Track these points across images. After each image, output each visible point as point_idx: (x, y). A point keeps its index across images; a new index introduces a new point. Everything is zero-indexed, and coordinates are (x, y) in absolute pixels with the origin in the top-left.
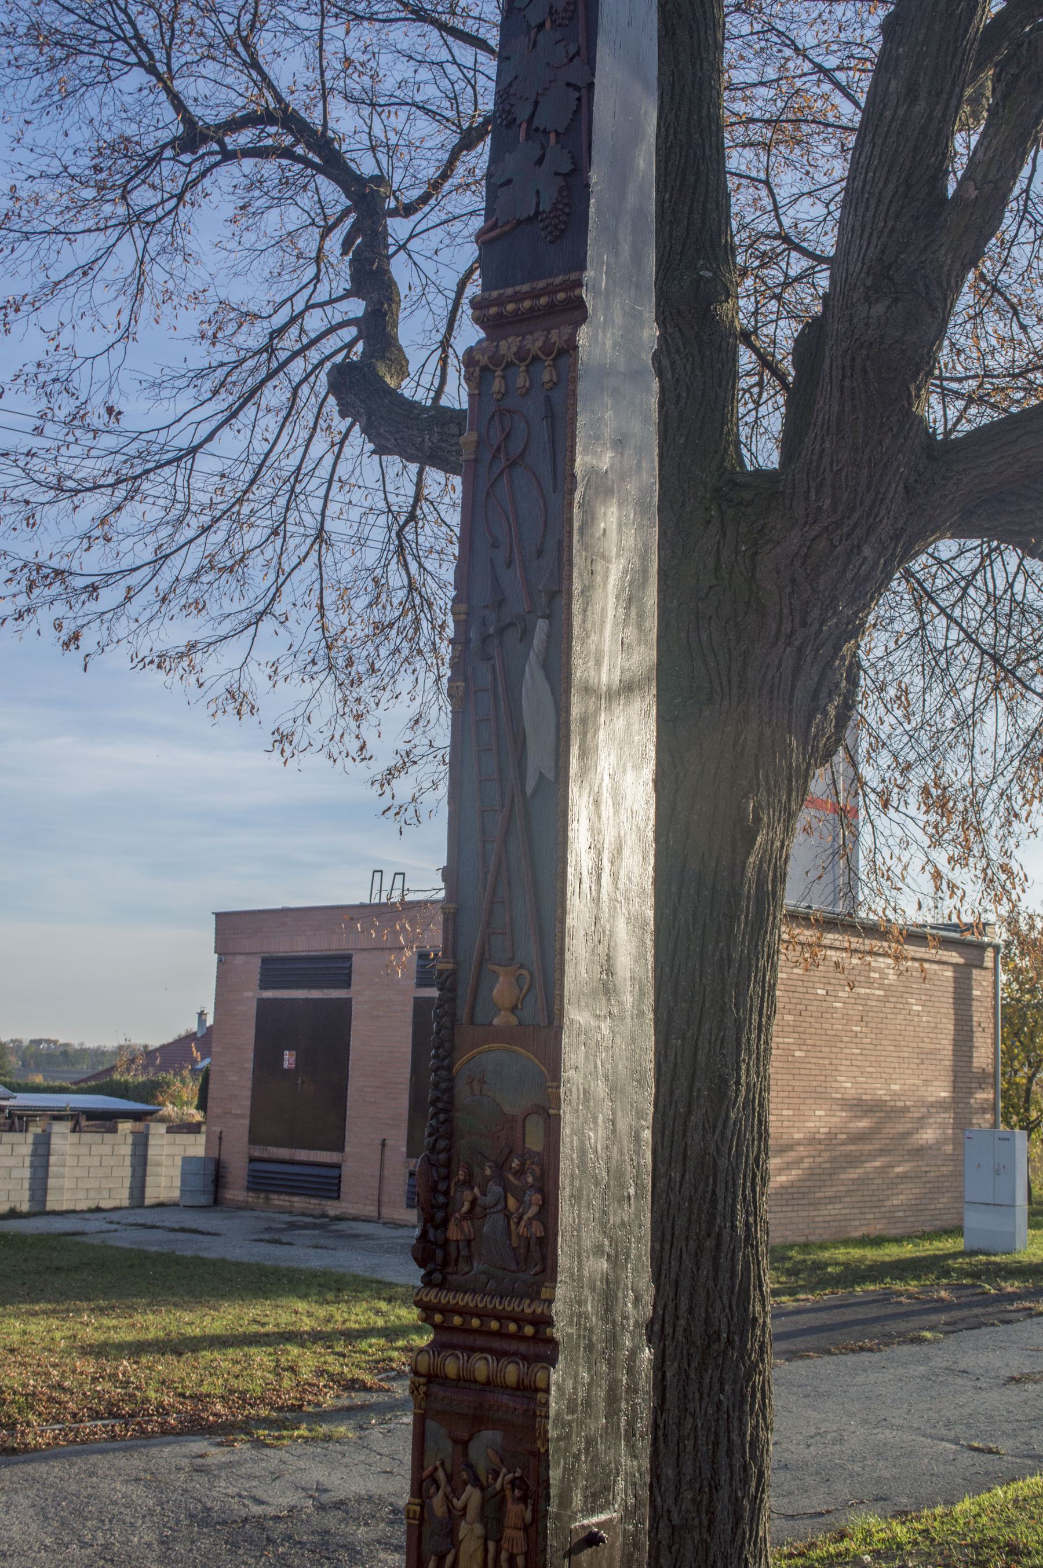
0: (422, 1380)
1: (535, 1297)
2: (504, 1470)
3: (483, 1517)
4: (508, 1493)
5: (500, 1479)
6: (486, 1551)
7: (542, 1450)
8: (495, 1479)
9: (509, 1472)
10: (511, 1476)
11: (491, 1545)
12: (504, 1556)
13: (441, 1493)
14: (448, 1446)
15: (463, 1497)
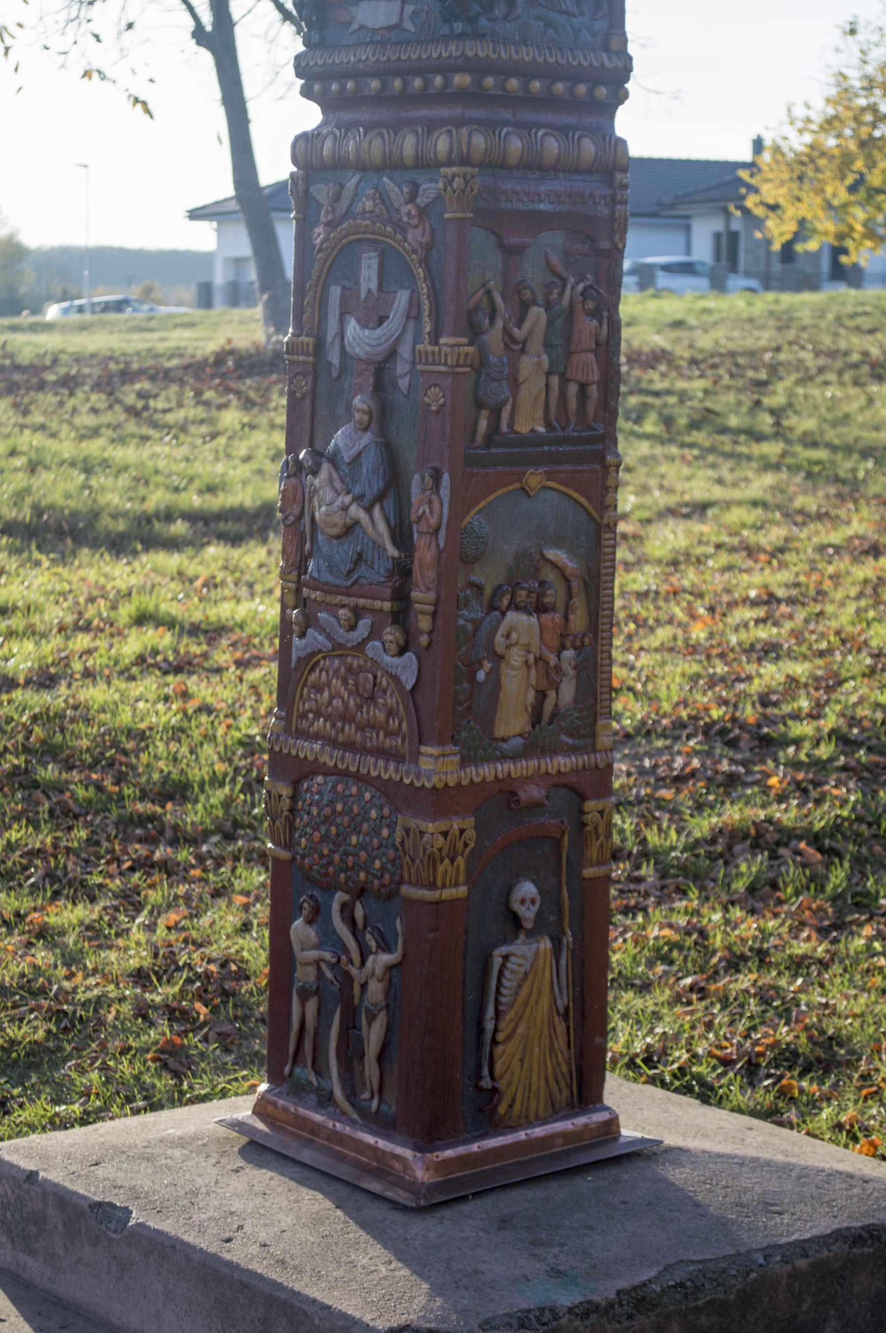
0: (476, 170)
1: (606, 48)
2: (572, 280)
3: (548, 346)
4: (579, 307)
5: (568, 292)
6: (547, 386)
7: (620, 246)
8: (562, 293)
9: (577, 283)
10: (581, 286)
11: (555, 380)
12: (573, 389)
13: (500, 323)
14: (496, 258)
15: (527, 324)
